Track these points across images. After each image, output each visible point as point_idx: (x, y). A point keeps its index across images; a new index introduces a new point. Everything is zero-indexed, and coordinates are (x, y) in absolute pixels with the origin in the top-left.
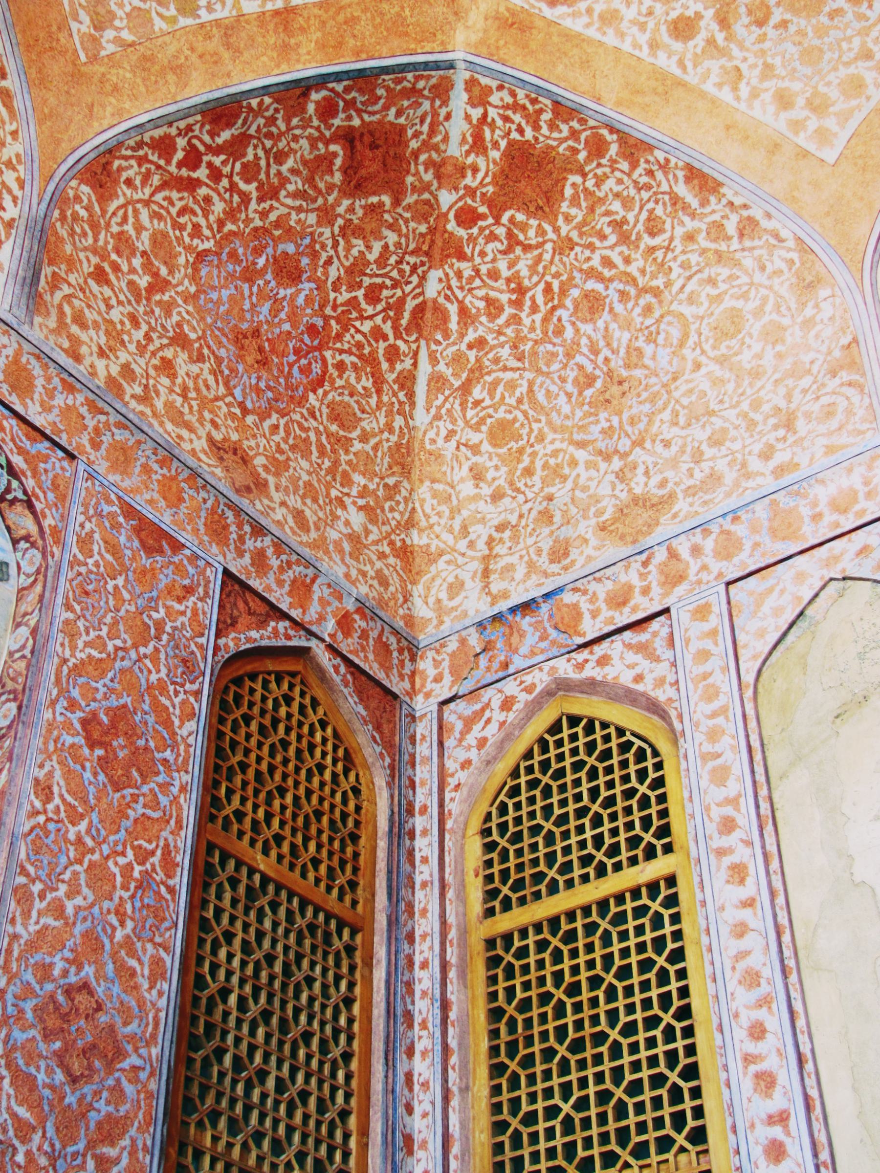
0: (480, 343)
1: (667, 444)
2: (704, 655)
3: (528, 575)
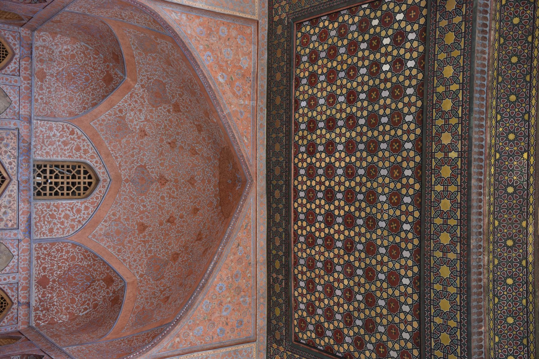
0: (90, 59)
1: (54, 84)
2: (7, 79)
3: (40, 54)
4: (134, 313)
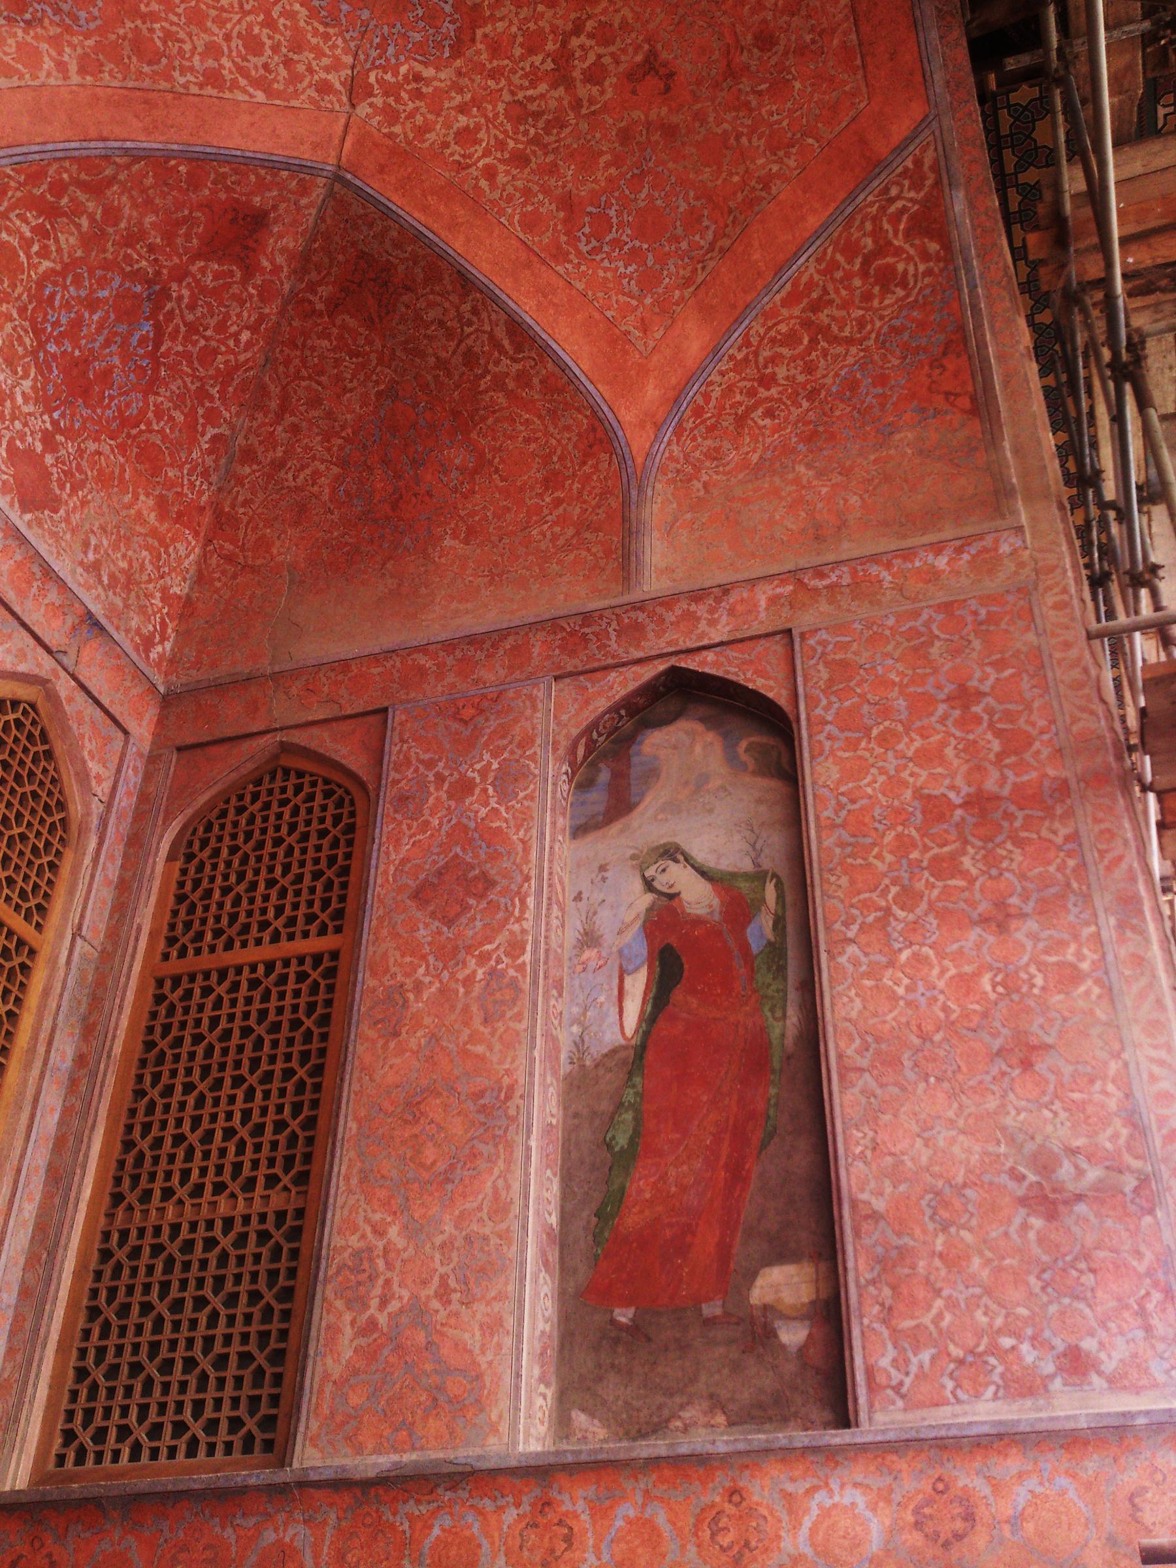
4: (560, 255)
